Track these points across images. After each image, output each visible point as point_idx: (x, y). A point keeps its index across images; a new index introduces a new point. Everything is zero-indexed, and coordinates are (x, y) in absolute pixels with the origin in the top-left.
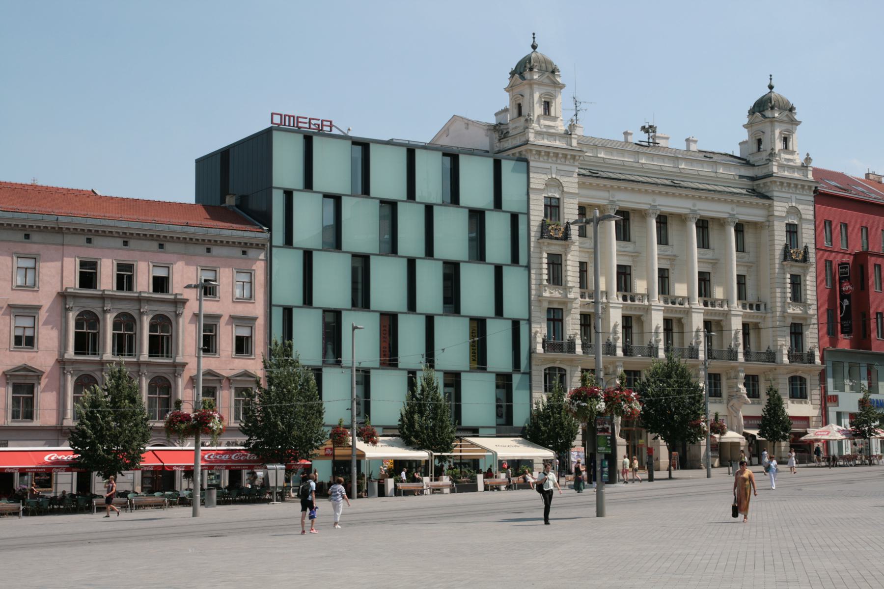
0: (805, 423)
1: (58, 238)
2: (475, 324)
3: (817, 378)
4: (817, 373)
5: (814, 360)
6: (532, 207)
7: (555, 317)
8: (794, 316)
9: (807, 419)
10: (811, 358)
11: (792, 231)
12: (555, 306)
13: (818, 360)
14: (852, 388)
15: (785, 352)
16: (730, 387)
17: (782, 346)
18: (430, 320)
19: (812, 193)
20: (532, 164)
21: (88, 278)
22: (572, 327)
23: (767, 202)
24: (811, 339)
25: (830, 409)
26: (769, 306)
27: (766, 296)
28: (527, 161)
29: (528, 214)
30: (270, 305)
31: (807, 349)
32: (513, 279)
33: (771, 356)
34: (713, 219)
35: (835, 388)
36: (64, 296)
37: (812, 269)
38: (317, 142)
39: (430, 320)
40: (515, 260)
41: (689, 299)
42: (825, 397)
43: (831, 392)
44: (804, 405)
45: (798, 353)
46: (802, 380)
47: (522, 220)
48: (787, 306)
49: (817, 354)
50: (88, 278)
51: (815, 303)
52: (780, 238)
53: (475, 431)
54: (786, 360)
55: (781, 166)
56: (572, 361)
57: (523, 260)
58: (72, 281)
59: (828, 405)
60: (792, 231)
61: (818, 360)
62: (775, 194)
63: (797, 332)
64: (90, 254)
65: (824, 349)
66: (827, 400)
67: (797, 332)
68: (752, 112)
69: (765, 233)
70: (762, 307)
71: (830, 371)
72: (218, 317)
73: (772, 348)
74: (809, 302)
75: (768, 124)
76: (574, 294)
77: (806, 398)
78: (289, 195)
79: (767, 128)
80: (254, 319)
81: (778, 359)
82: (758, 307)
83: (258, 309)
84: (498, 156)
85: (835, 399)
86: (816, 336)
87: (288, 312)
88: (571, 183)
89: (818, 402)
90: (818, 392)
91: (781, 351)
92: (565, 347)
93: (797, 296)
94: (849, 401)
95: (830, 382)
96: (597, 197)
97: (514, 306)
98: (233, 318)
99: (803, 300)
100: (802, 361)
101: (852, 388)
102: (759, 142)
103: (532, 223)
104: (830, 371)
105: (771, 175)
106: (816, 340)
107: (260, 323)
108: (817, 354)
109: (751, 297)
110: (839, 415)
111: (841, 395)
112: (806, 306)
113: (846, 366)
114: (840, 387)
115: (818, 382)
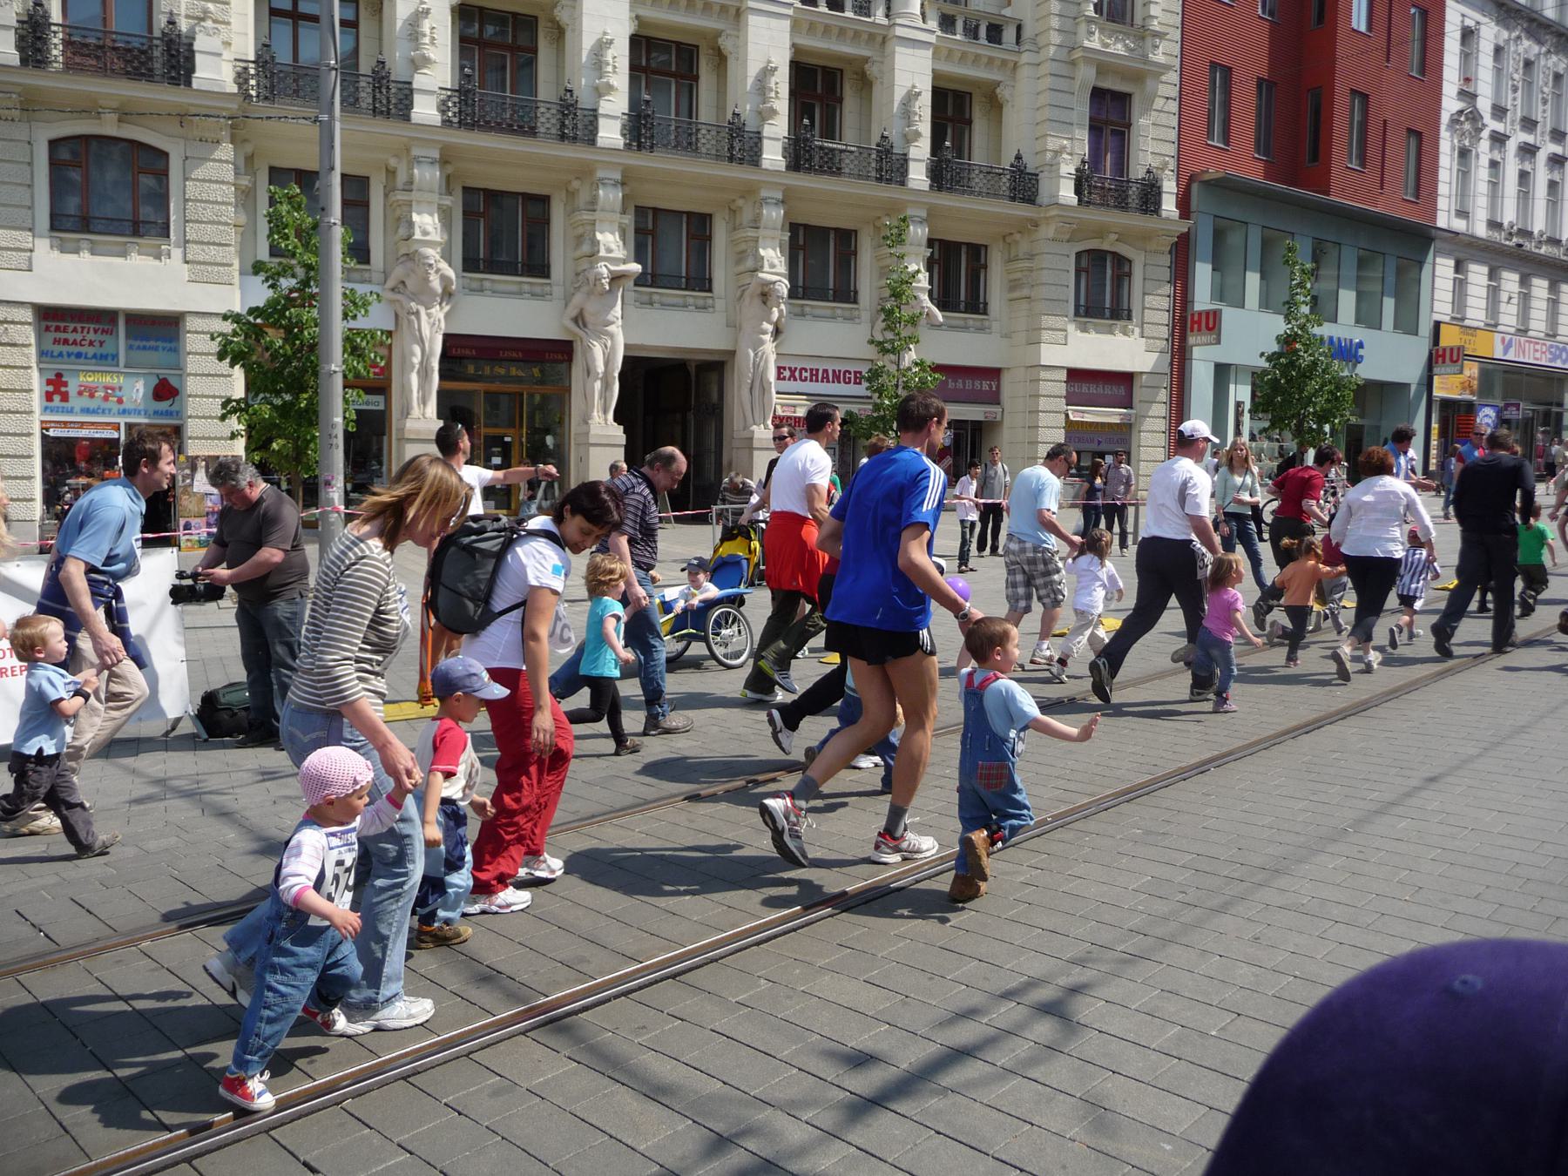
0: (1121, 391)
3: (1166, 260)
4: (1167, 243)
5: (1158, 204)
8: (1103, 68)
9: (1126, 379)
10: (1150, 196)
13: (1169, 205)
14: (1266, 303)
15: (1068, 168)
16: (884, 272)
17: (1057, 153)
24: (1154, 144)
25: (1197, 352)
26: (1027, 33)
27: (1022, 8)
31: (1137, 172)
33: (1023, 185)
35: (1220, 293)
42: (1183, 319)
43: (1202, 299)
44: (1120, 337)
45: (1109, 179)
46: (1122, 266)
48: (1083, 28)
49: (1169, 186)
51: (1177, 35)
53: (56, 388)
54: (1067, 193)
56: (183, 117)
59: (1191, 340)
61: (1169, 205)
63: (1111, 114)
65: (1191, 179)
66: (1188, 324)
67: (1111, 114)
70: (1009, 35)
71: (1204, 242)
74: (1155, 25)
77: (1129, 318)
81: (1044, 196)
82: (995, 33)
85: (1211, 323)
86: (1173, 135)
89: (1164, 332)
90: (1165, 303)
91: (1054, 166)
94: (1251, 333)
95: (1203, 273)
99: (1138, 20)
100: (1122, 204)
101: (1266, 303)
106: (1171, 150)
108: (1169, 186)
110: (1223, 373)
111: (1229, 315)
112: (1144, 35)
114: (1228, 293)
115: (1166, 274)
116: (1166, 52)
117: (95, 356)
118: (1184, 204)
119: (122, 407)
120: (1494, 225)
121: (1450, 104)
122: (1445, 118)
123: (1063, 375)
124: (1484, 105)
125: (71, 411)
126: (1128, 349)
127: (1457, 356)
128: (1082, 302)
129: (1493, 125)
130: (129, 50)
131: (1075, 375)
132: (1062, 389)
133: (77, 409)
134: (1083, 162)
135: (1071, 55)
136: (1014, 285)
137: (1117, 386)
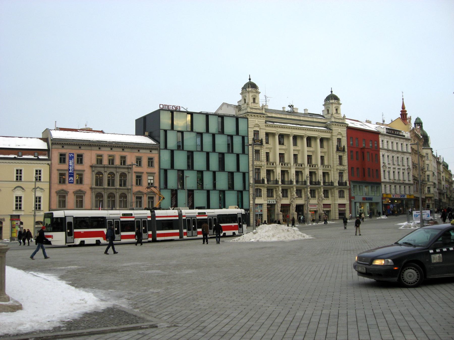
1: (90, 148)
2: (230, 175)
7: (258, 171)
9: (345, 204)
11: (339, 140)
12: (258, 168)
13: (348, 184)
18: (214, 173)
21: (99, 161)
22: (263, 175)
23: (331, 131)
26: (332, 166)
28: (248, 119)
29: (248, 136)
30: (160, 169)
32: (243, 159)
34: (270, 133)
36: (92, 167)
37: (346, 154)
38: (175, 113)
39: (214, 173)
40: (244, 152)
46: (343, 191)
47: (246, 138)
49: (348, 183)
50: (99, 161)
52: (335, 143)
56: (264, 186)
57: (246, 152)
58: (94, 162)
60: (339, 140)
61: (348, 184)
63: (341, 174)
64: (100, 152)
67: (341, 174)
69: (331, 142)
72: (143, 173)
73: (333, 181)
76: (264, 163)
78: (166, 131)
80: (155, 173)
83: (155, 169)
85: (354, 198)
87: (166, 171)
88: (262, 125)
93: (341, 164)
97: (243, 168)
98: (147, 173)
102: (328, 110)
104: (352, 189)
107: (157, 174)
108: (348, 183)
109: (326, 163)
110: (355, 203)
113: (358, 186)
116: (346, 168)
118: (349, 184)
120: (390, 179)
121: (382, 165)
122: (381, 167)
124: (387, 164)
126: (345, 201)
127: (385, 198)
129: (388, 166)
131: (339, 204)
135: (337, 170)
136: (331, 194)
137: (344, 205)
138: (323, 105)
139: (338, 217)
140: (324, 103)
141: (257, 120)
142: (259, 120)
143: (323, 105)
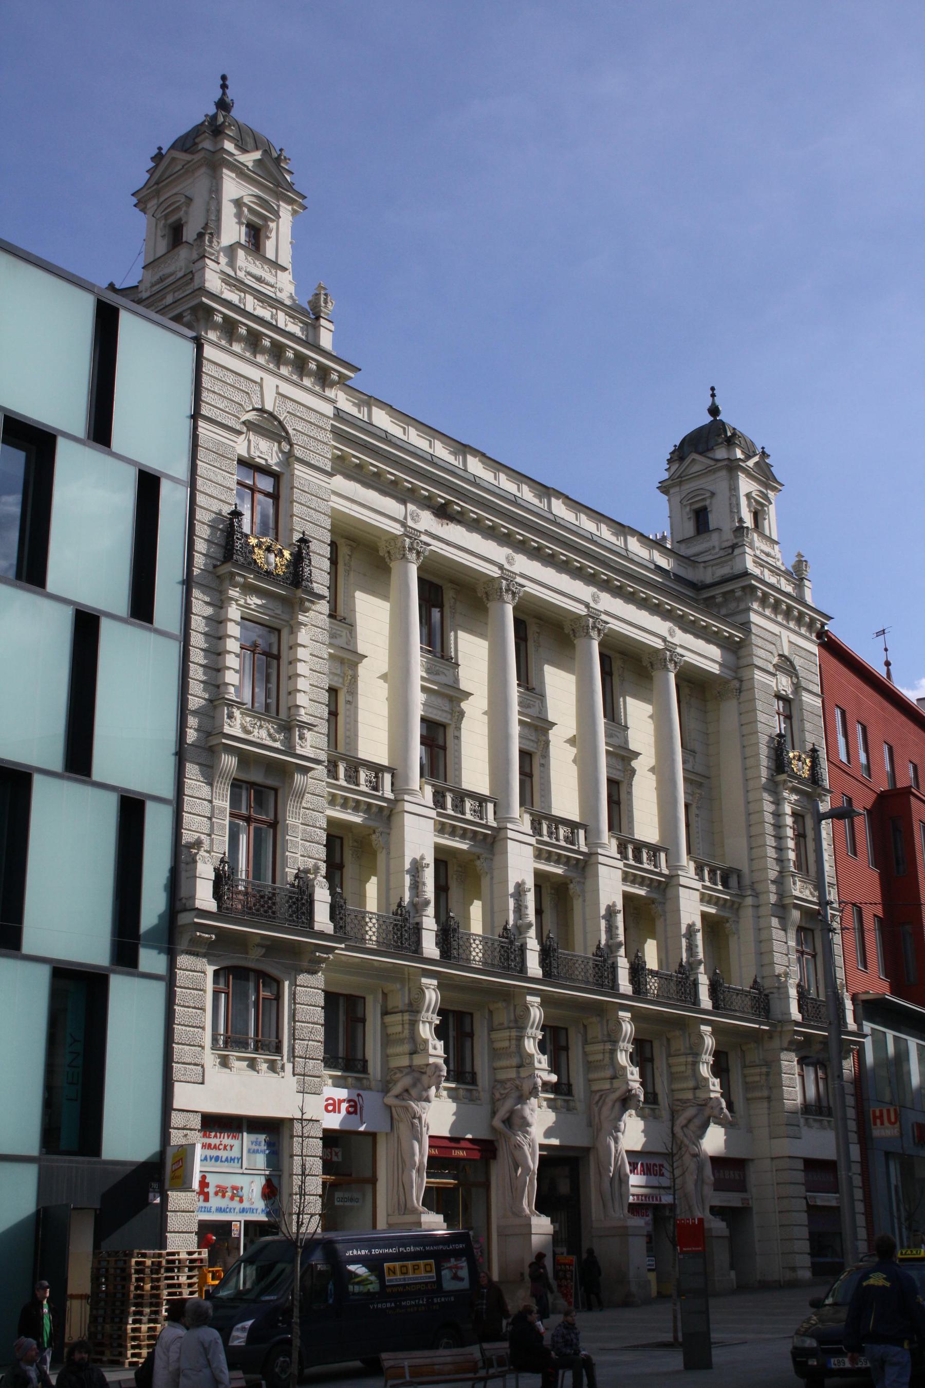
6: (201, 467)
11: (789, 706)
19: (814, 637)
20: (209, 352)
41: (585, 826)
55: (759, 562)
60: (789, 706)
62: (754, 618)
68: (679, 454)
69: (729, 710)
75: (723, 473)
79: (719, 483)
84: (112, 299)
88: (319, 447)
92: (282, 907)
96: (380, 512)
103: (200, 515)
105: (746, 574)
117: (227, 1160)
119: (242, 1206)
123: (801, 1166)
125: (209, 1211)
128: (222, 1030)
130: (262, 897)
132: (800, 1176)
133: (213, 1209)
134: (222, 861)
138: (664, 488)
139: (806, 1261)
140: (666, 475)
141: (271, 382)
142: (287, 389)
143: (664, 488)
